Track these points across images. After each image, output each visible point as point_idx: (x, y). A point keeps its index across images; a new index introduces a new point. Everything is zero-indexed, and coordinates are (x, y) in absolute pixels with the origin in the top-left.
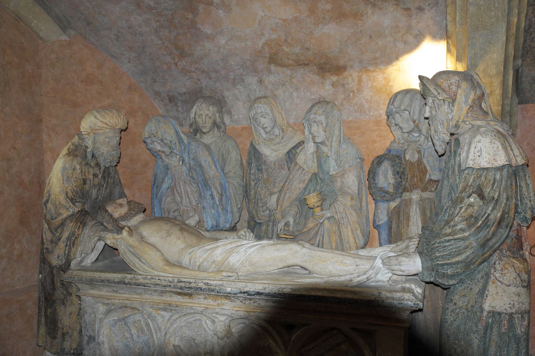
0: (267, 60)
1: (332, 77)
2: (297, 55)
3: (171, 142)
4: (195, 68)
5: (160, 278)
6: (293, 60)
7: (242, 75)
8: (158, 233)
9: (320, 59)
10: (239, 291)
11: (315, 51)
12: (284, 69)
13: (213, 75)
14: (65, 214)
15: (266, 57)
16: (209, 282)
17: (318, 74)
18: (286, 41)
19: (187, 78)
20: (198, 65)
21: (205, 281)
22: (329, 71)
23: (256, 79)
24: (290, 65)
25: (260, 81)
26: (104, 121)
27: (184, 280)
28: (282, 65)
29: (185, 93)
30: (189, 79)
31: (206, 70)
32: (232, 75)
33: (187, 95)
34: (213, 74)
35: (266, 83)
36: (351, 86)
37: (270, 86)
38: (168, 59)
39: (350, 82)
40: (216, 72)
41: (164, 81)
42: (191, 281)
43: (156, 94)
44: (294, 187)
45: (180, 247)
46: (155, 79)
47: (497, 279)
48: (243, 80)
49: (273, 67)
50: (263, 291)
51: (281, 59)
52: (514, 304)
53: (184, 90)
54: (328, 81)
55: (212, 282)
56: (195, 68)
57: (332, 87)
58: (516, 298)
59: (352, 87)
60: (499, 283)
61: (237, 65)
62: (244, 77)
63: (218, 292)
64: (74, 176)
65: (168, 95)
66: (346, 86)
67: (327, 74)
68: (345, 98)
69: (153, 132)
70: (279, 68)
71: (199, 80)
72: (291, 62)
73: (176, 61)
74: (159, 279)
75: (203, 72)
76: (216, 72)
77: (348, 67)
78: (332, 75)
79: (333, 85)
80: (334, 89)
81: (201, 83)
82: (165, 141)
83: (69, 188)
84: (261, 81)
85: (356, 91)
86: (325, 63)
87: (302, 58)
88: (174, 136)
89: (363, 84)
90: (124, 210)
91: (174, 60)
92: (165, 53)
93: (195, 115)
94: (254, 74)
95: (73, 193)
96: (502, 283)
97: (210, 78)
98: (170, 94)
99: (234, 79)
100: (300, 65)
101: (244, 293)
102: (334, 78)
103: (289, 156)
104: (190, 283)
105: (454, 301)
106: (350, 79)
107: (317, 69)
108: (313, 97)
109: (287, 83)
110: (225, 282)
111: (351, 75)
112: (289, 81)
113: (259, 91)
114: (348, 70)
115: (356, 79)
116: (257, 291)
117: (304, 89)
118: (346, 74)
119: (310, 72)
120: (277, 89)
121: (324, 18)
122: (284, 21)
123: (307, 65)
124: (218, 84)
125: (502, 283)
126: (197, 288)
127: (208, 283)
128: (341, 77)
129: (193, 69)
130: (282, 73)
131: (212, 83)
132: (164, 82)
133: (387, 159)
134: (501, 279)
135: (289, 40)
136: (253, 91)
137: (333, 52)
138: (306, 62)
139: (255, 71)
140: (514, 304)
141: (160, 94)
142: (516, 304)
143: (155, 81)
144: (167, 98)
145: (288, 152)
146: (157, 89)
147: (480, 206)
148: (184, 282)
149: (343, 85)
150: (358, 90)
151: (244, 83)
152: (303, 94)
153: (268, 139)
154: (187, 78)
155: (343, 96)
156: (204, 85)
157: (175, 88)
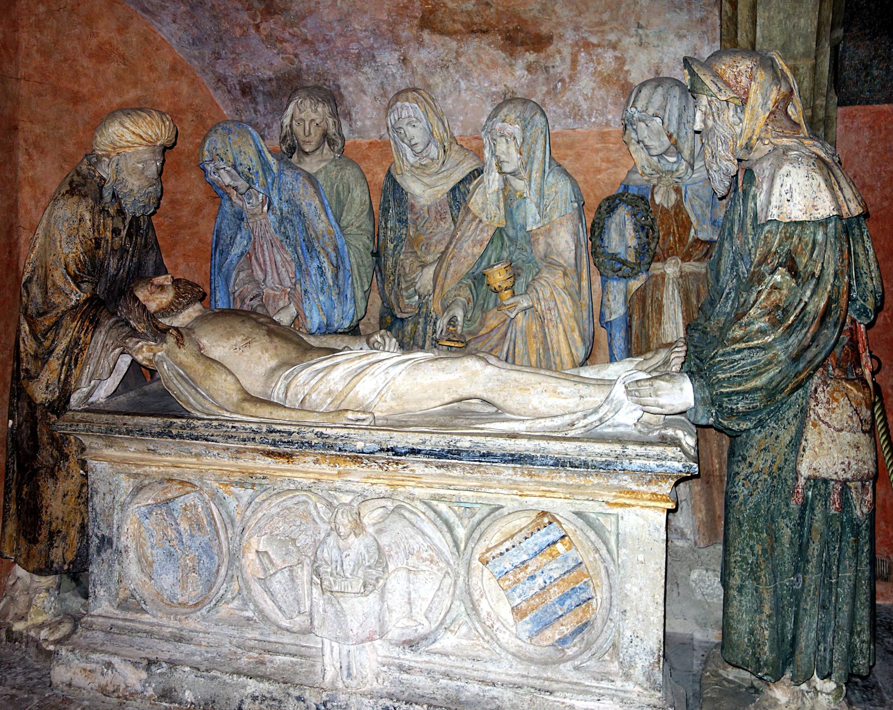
1: (527, 54)
3: (249, 169)
4: (290, 34)
5: (236, 424)
6: (462, 23)
7: (372, 48)
10: (378, 448)
12: (447, 38)
13: (322, 47)
16: (324, 430)
17: (503, 48)
19: (275, 51)
20: (295, 29)
21: (317, 430)
22: (522, 44)
23: (396, 55)
24: (456, 33)
27: (279, 428)
28: (442, 32)
30: (278, 54)
31: (309, 38)
32: (354, 48)
34: (322, 45)
35: (414, 62)
36: (559, 70)
37: (420, 70)
39: (557, 64)
40: (328, 42)
41: (234, 56)
42: (292, 429)
46: (218, 53)
47: (820, 419)
48: (374, 57)
49: (426, 35)
50: (422, 447)
52: (849, 463)
54: (520, 61)
55: (329, 432)
56: (290, 34)
57: (526, 73)
58: (853, 453)
59: (561, 73)
60: (823, 426)
61: (365, 31)
66: (551, 71)
67: (519, 48)
68: (548, 93)
70: (436, 37)
71: (296, 56)
72: (458, 26)
74: (233, 427)
75: (305, 41)
76: (328, 42)
77: (555, 37)
78: (527, 50)
79: (529, 68)
80: (530, 76)
81: (300, 62)
82: (240, 168)
83: (71, 255)
84: (404, 61)
85: (567, 80)
86: (516, 30)
88: (255, 159)
89: (579, 68)
93: (291, 121)
94: (394, 47)
95: (77, 265)
96: (829, 426)
97: (316, 53)
99: (359, 55)
100: (473, 32)
101: (388, 450)
102: (531, 57)
104: (290, 433)
105: (749, 460)
106: (558, 57)
107: (502, 39)
108: (494, 89)
110: (352, 431)
111: (559, 52)
112: (454, 61)
113: (402, 77)
114: (555, 42)
115: (568, 59)
116: (411, 446)
118: (552, 48)
119: (489, 45)
120: (433, 74)
123: (485, 32)
124: (329, 64)
125: (829, 426)
126: (302, 443)
127: (322, 433)
128: (543, 55)
129: (287, 36)
130: (443, 45)
131: (320, 62)
134: (827, 419)
136: (391, 78)
138: (485, 27)
139: (396, 41)
140: (849, 463)
142: (853, 462)
143: (217, 56)
147: (790, 289)
148: (279, 431)
150: (570, 77)
151: (376, 62)
152: (476, 83)
153: (417, 165)
154: (275, 51)
155: (545, 89)
156: (304, 66)
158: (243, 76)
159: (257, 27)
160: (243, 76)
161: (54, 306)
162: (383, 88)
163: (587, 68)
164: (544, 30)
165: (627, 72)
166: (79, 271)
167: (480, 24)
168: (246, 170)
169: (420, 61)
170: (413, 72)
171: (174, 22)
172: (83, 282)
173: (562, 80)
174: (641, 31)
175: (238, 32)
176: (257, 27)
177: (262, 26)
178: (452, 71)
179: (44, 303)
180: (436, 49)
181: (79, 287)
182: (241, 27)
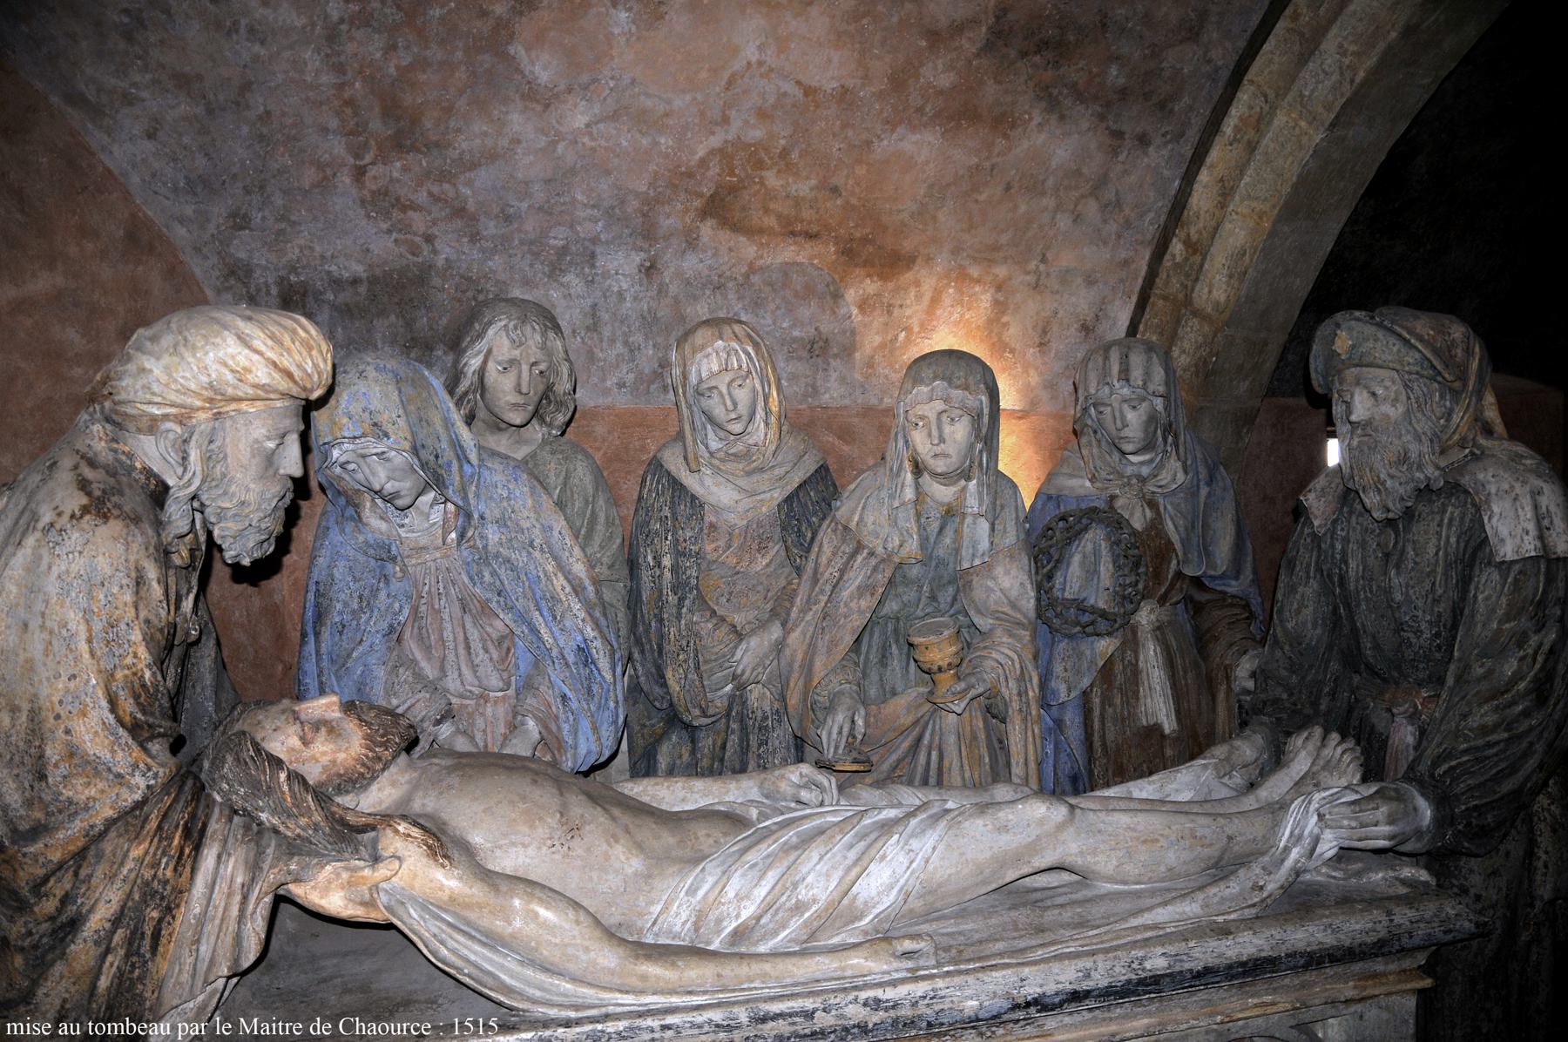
0: (698, 203)
1: (868, 281)
2: (797, 202)
4: (430, 194)
6: (779, 217)
7: (595, 240)
8: (533, 827)
9: (857, 226)
11: (854, 201)
12: (742, 239)
13: (490, 228)
14: (104, 802)
15: (700, 195)
18: (784, 153)
19: (385, 226)
20: (446, 186)
22: (867, 263)
23: (638, 258)
24: (761, 231)
25: (651, 267)
26: (285, 362)
28: (737, 228)
29: (355, 281)
30: (389, 232)
31: (471, 206)
32: (558, 237)
33: (363, 289)
34: (492, 224)
35: (667, 276)
37: (673, 289)
38: (337, 147)
40: (508, 219)
41: (283, 225)
43: (232, 273)
44: (842, 609)
45: (630, 871)
46: (245, 216)
48: (593, 256)
49: (707, 229)
51: (744, 209)
53: (359, 269)
56: (430, 194)
59: (909, 317)
61: (594, 206)
62: (599, 250)
63: (930, 1025)
64: (142, 615)
65: (281, 281)
66: (896, 312)
67: (857, 270)
68: (882, 346)
69: (378, 419)
70: (725, 235)
71: (429, 239)
72: (771, 221)
73: (368, 158)
75: (459, 212)
76: (508, 219)
78: (870, 276)
81: (435, 252)
82: (422, 453)
83: (119, 675)
84: (650, 270)
85: (916, 329)
86: (865, 240)
87: (807, 214)
90: (351, 746)
91: (357, 156)
92: (334, 123)
93: (485, 362)
94: (639, 243)
95: (136, 697)
97: (475, 238)
98: (293, 278)
99: (564, 251)
100: (793, 233)
103: (791, 509)
107: (836, 252)
108: (796, 333)
109: (730, 285)
113: (635, 298)
117: (778, 308)
120: (695, 298)
121: (920, 110)
122: (809, 91)
123: (811, 236)
124: (496, 263)
128: (891, 285)
129: (422, 197)
130: (730, 250)
131: (476, 255)
132: (280, 232)
133: (1101, 521)
135: (795, 155)
136: (614, 299)
137: (899, 211)
138: (815, 228)
139: (648, 233)
141: (249, 271)
143: (239, 221)
144: (274, 291)
145: (788, 499)
146: (242, 255)
149: (889, 309)
150: (922, 326)
151: (593, 266)
152: (769, 321)
153: (721, 454)
154: (385, 226)
155: (878, 339)
156: (440, 261)
157: (323, 257)
158: (293, 269)
159: (360, 173)
160: (293, 269)
161: (72, 809)
162: (594, 315)
163: (951, 314)
164: (907, 245)
165: (1006, 325)
166: (144, 713)
167: (810, 223)
168: (432, 458)
169: (679, 274)
170: (660, 291)
171: (151, 136)
172: (152, 738)
173: (908, 329)
174: (1042, 267)
175: (309, 176)
176: (360, 173)
177: (373, 171)
178: (731, 296)
179: (29, 803)
180: (715, 255)
181: (145, 750)
182: (321, 167)
